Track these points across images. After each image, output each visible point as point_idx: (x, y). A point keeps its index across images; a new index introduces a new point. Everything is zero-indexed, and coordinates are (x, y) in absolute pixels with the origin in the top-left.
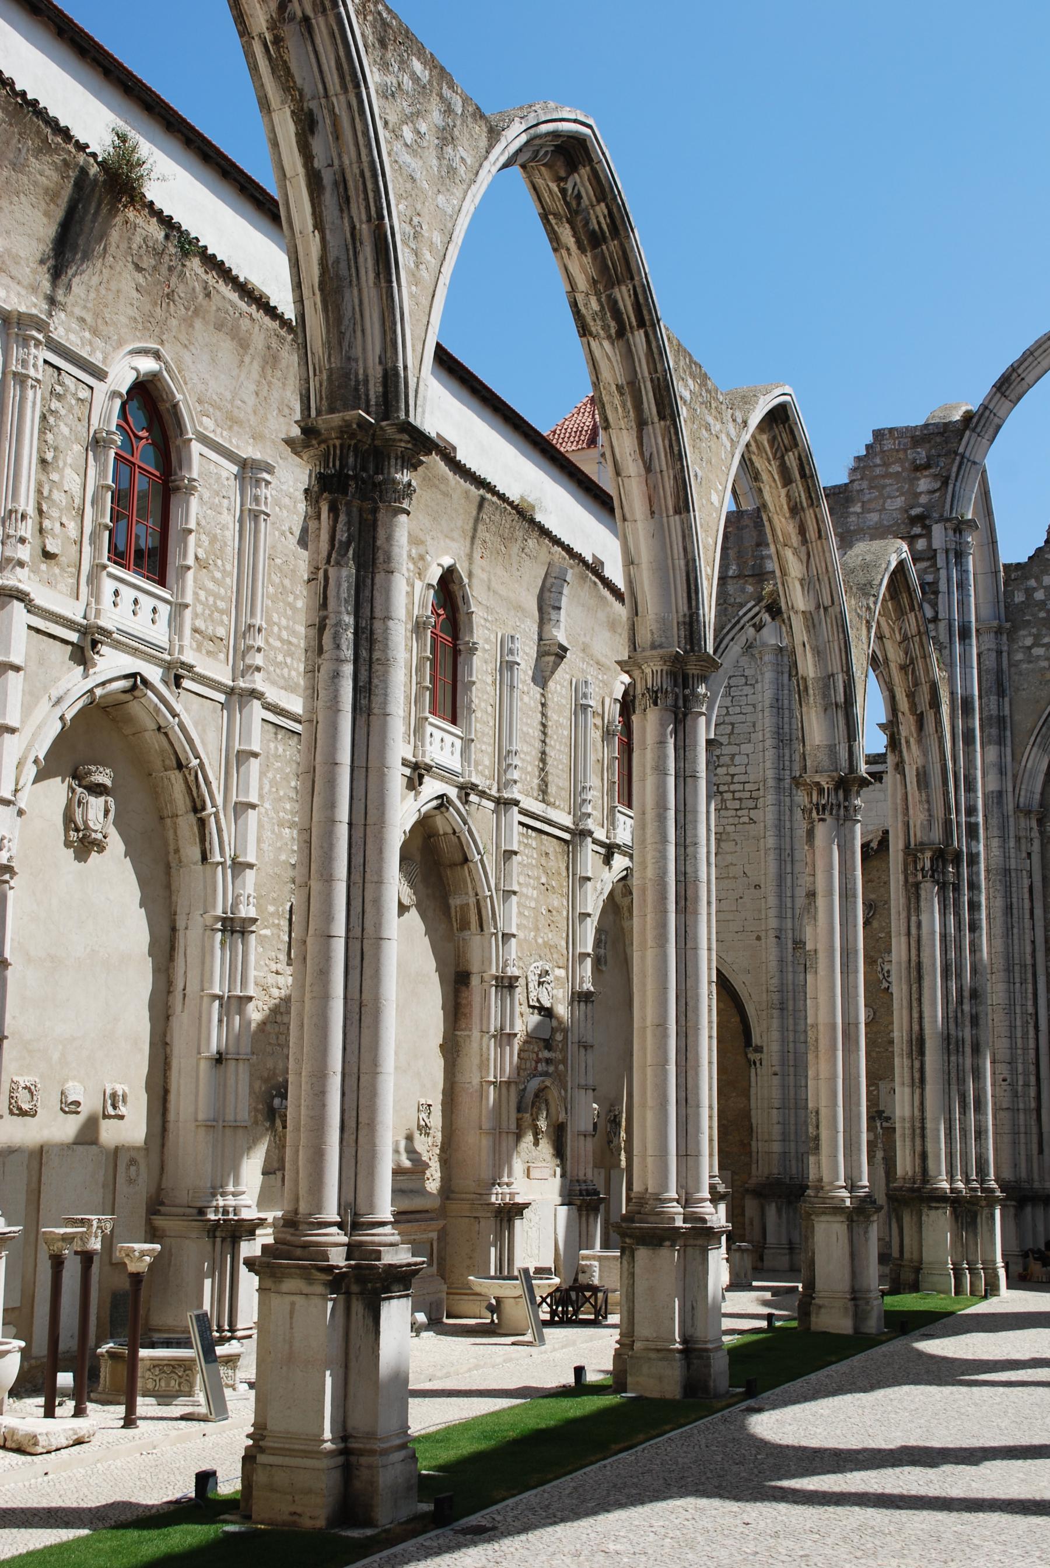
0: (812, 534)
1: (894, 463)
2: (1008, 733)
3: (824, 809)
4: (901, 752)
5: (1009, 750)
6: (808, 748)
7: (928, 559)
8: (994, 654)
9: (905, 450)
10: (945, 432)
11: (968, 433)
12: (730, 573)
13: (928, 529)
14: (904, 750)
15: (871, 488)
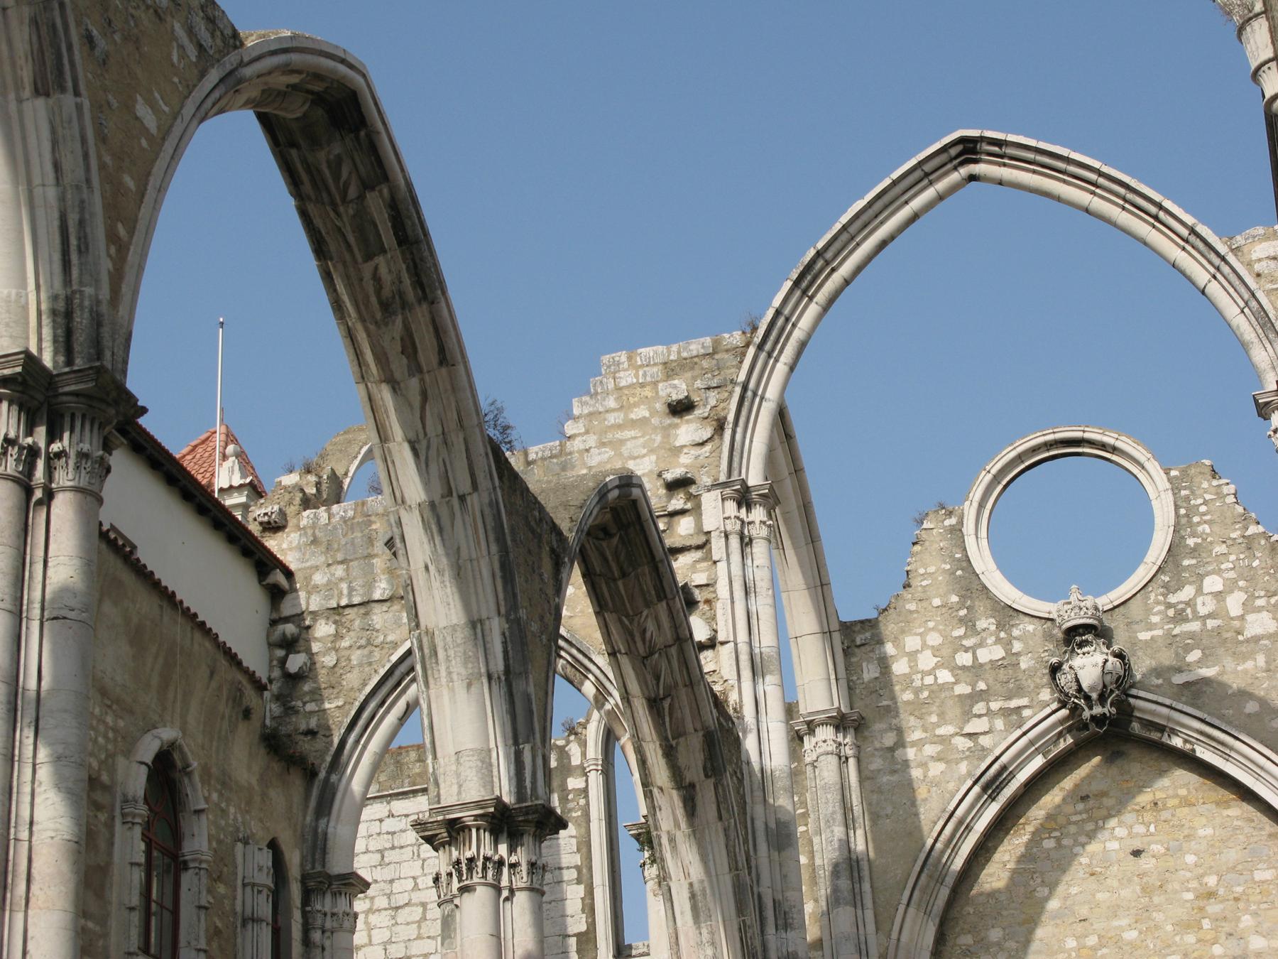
0: (428, 354)
1: (636, 405)
2: (866, 886)
3: (470, 869)
4: (662, 860)
5: (869, 914)
6: (441, 760)
7: (699, 547)
8: (833, 760)
9: (655, 384)
10: (715, 352)
11: (751, 351)
12: (377, 596)
13: (697, 498)
14: (668, 855)
15: (603, 444)
